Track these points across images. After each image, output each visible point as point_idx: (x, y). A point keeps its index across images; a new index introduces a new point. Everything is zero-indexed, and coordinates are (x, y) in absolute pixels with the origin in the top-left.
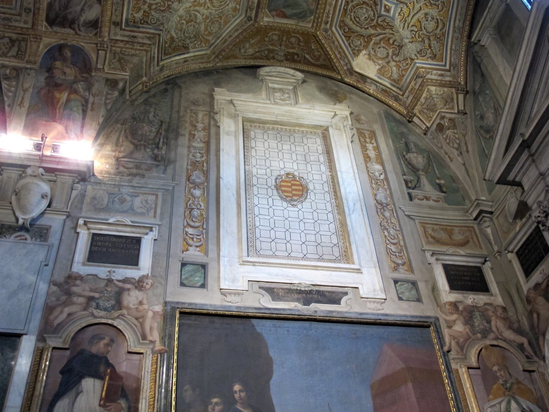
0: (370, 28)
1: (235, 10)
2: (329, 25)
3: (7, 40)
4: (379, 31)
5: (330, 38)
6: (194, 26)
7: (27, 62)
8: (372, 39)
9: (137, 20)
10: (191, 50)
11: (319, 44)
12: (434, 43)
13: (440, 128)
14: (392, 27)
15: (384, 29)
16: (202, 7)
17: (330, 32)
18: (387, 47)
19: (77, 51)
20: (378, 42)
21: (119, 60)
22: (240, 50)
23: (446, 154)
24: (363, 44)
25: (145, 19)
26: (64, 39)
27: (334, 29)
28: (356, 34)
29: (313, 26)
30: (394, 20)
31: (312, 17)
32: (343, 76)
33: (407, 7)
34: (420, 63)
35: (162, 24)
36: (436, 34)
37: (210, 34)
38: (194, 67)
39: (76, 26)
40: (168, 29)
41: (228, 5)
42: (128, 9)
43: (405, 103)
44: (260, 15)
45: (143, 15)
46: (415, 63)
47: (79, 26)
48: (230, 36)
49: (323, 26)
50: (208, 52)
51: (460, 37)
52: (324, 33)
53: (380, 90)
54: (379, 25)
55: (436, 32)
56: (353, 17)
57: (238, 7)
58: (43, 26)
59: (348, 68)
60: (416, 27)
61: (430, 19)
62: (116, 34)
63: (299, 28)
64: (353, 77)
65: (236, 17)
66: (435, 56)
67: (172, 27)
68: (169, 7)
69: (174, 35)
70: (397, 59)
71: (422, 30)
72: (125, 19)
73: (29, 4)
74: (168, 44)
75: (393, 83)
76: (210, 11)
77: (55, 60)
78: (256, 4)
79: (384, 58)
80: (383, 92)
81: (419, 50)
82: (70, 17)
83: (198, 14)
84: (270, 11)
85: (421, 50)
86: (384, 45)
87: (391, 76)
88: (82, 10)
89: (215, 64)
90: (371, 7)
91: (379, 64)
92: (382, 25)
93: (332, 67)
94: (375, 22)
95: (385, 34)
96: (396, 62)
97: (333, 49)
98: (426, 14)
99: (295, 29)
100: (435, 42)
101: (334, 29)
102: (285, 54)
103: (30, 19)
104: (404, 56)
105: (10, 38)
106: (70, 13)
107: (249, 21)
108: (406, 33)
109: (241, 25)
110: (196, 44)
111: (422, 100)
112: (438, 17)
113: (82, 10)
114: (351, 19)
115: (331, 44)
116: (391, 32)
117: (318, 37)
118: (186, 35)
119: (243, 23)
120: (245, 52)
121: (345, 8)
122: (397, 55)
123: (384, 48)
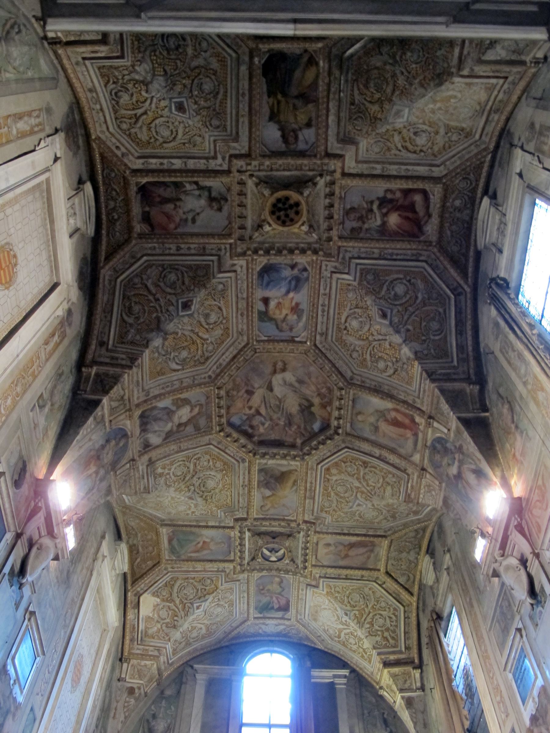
1: (169, 513)
3: (122, 393)
7: (111, 421)
9: (156, 471)
12: (184, 643)
13: (131, 691)
14: (186, 615)
15: (183, 610)
21: (125, 481)
23: (116, 709)
26: (132, 434)
27: (169, 574)
29: (167, 560)
31: (174, 558)
35: (157, 489)
43: (133, 648)
44: (168, 528)
49: (169, 566)
58: (138, 413)
62: (142, 464)
68: (169, 486)
70: (164, 628)
73: (153, 392)
77: (115, 439)
82: (149, 427)
84: (172, 532)
87: (149, 628)
91: (153, 615)
94: (186, 601)
98: (201, 629)
103: (142, 399)
105: (124, 395)
108: (186, 626)
109: (155, 516)
111: (143, 663)
113: (156, 432)
122: (167, 627)
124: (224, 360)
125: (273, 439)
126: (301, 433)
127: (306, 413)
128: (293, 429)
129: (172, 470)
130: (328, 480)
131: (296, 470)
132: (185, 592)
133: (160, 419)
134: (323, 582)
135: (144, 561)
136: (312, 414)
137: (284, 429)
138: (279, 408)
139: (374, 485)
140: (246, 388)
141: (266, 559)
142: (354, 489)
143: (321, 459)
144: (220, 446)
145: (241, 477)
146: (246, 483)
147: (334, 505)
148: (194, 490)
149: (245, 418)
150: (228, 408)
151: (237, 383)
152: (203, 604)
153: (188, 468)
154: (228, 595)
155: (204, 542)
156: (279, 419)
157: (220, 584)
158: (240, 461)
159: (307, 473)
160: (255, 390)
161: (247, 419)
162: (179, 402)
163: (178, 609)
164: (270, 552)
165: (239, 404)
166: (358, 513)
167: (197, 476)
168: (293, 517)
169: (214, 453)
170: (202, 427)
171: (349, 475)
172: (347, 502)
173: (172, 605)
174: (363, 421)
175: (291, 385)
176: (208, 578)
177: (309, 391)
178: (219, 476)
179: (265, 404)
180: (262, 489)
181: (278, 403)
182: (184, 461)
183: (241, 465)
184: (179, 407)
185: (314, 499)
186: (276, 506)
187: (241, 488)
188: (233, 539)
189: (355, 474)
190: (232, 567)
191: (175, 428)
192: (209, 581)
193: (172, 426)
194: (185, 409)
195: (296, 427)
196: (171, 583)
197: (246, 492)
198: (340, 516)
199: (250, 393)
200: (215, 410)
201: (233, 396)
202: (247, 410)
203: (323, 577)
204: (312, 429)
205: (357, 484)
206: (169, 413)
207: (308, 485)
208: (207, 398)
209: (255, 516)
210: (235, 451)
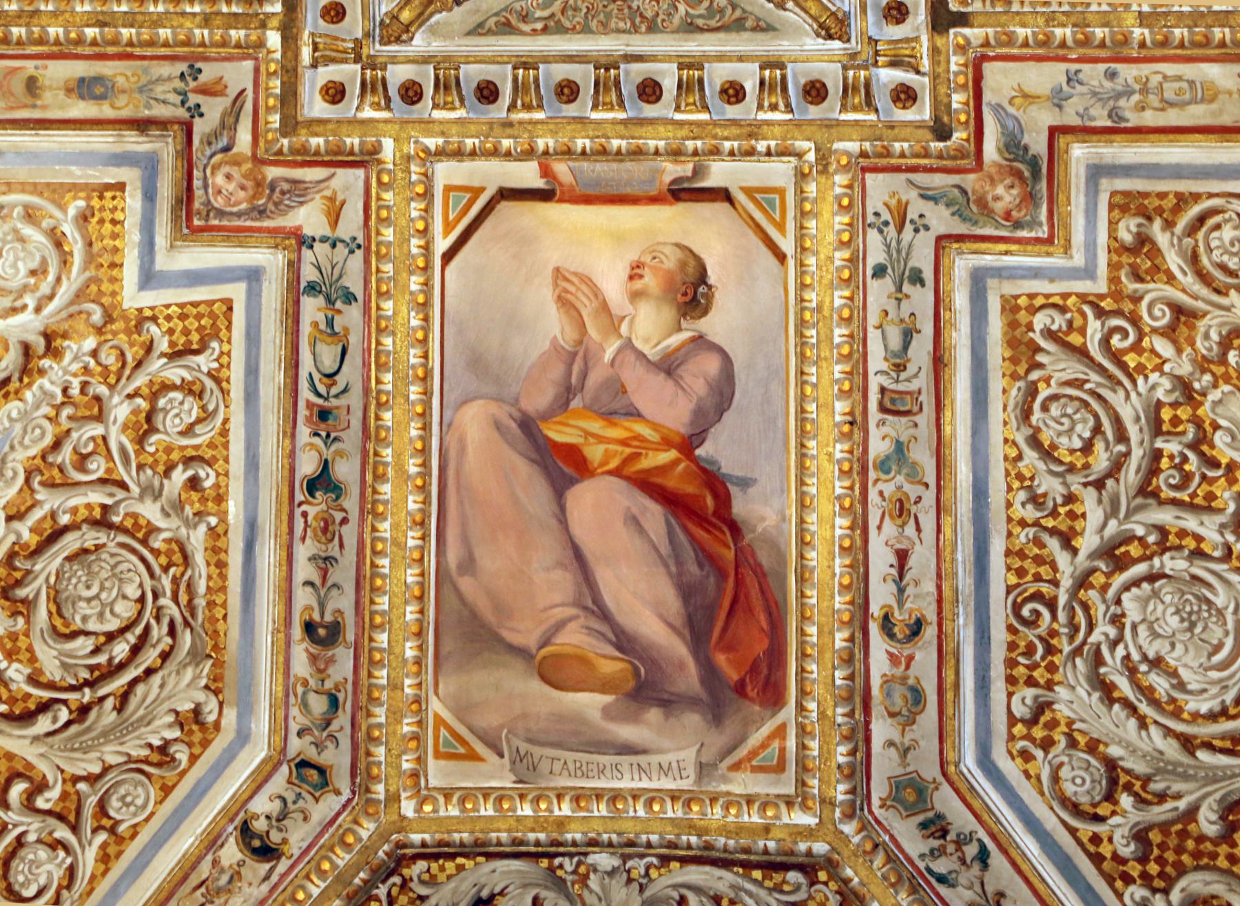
134: (253, 276)
203: (294, 267)
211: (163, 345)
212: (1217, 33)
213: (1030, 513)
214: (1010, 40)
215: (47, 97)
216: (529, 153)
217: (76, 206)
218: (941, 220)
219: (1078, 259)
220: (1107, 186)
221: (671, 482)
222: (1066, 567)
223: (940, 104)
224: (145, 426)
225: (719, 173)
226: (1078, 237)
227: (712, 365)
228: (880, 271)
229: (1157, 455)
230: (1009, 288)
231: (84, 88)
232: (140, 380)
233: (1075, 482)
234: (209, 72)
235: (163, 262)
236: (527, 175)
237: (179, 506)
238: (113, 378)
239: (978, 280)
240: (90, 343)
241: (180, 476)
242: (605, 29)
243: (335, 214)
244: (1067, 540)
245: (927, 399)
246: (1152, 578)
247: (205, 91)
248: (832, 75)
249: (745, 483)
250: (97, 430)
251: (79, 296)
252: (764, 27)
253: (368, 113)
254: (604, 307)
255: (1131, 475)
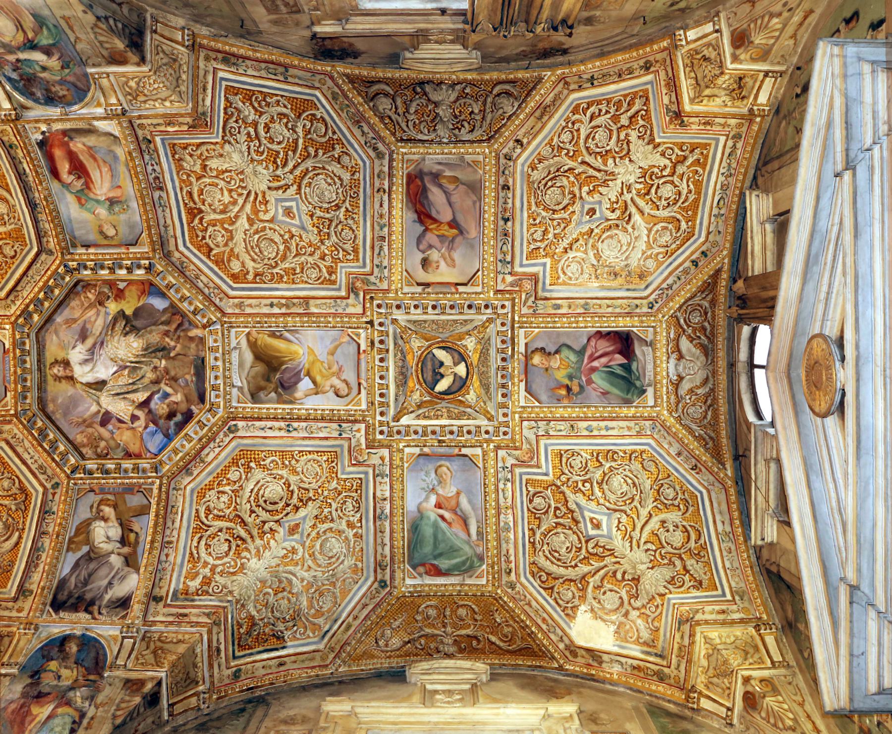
0: (579, 565)
1: (355, 570)
2: (513, 574)
4: (597, 565)
5: (523, 597)
6: (289, 600)
8: (588, 583)
9: (192, 590)
10: (289, 644)
11: (507, 611)
12: (690, 563)
14: (612, 552)
16: (299, 567)
17: (518, 587)
18: (615, 588)
19: (88, 643)
20: (600, 584)
22: (376, 642)
24: (577, 595)
25: (205, 588)
27: (523, 579)
28: (561, 580)
29: (488, 581)
30: (611, 539)
32: (562, 662)
33: (628, 516)
34: (675, 597)
36: (690, 549)
37: (319, 613)
38: (299, 674)
39: (96, 608)
40: (240, 600)
41: (343, 561)
42: (179, 576)
44: (399, 575)
45: (202, 582)
46: (669, 599)
47: (100, 608)
48: (355, 618)
49: (505, 578)
50: (321, 646)
51: (733, 548)
52: (509, 590)
53: (629, 670)
54: (591, 554)
55: (689, 546)
56: (547, 553)
57: (360, 565)
59: (566, 646)
60: (652, 543)
61: (671, 528)
63: (466, 588)
64: (579, 659)
65: (360, 583)
66: (701, 583)
67: (249, 597)
69: (254, 613)
70: (638, 604)
71: (664, 547)
72: (174, 592)
74: (245, 627)
75: (645, 649)
76: (313, 573)
78: (388, 558)
79: (618, 609)
80: (636, 672)
81: (668, 578)
83: (294, 579)
84: (414, 567)
85: (673, 578)
86: (610, 586)
87: (639, 637)
88: (110, 584)
89: (337, 670)
90: (570, 528)
91: (613, 623)
92: (596, 554)
93: (540, 650)
94: (584, 551)
95: (606, 566)
96: (638, 609)
97: (532, 615)
98: (663, 522)
99: (460, 591)
100: (693, 562)
101: (523, 579)
102: (455, 640)
104: (647, 593)
106: (91, 590)
107: (383, 587)
110: (296, 632)
112: (685, 523)
113: (110, 584)
114: (547, 558)
115: (526, 607)
116: (614, 560)
117: (500, 598)
118: (277, 614)
119: (374, 592)
120: (387, 645)
121: (532, 540)
123: (611, 591)
124: (36, 461)
125: (194, 379)
126: (176, 329)
127: (138, 323)
128: (172, 344)
129: (210, 560)
130: (256, 275)
131: (248, 334)
132: (563, 551)
133: (90, 575)
135: (495, 628)
136: (137, 312)
137: (173, 358)
138: (135, 368)
139: (226, 193)
140: (96, 426)
141: (461, 384)
142: (255, 227)
143: (216, 291)
144: (195, 473)
145: (270, 433)
146: (282, 424)
147: (310, 259)
148: (276, 522)
149: (152, 427)
150: (128, 455)
151: (85, 440)
152: (587, 514)
153: (220, 530)
154: (577, 462)
155: (439, 506)
156: (155, 368)
157: (545, 478)
158: (232, 436)
159: (250, 314)
160: (103, 411)
161: (155, 423)
162: (75, 540)
163: (602, 568)
164: (442, 376)
165: (125, 437)
166: (319, 213)
167: (246, 518)
168: (358, 335)
169: (207, 482)
170: (145, 502)
171: (231, 238)
172: (292, 237)
173: (593, 581)
174: (115, 227)
175: (91, 351)
176: (531, 501)
177: (98, 322)
178: (258, 474)
179: (128, 393)
180: (298, 394)
181: (126, 372)
182: (201, 538)
183: (239, 434)
184: (88, 541)
185: (307, 299)
186: (335, 368)
187: (294, 434)
188: (426, 450)
189: (226, 230)
190: (501, 453)
191: (126, 550)
192: (537, 500)
193: (119, 554)
194: (96, 529)
195: (167, 339)
196: (544, 578)
197: (304, 424)
198: (335, 246)
199: (106, 419)
200: (114, 478)
201: (108, 447)
202: (136, 424)
204: (165, 310)
205: (242, 223)
206: (93, 557)
207: (276, 310)
208: (92, 490)
209: (364, 406)
210: (212, 445)
211: (541, 250)
212: (314, 319)
213: (354, 216)
214: (357, 318)
215: (567, 304)
216: (460, 293)
217: (560, 281)
218: (372, 279)
219: (344, 270)
220: (337, 286)
221: (430, 221)
222: (347, 204)
223: (372, 304)
224: (545, 232)
225: (419, 289)
226: (343, 275)
227: (421, 247)
228: (385, 267)
229: (328, 229)
230: (358, 264)
231: (558, 307)
232: (546, 242)
233: (345, 223)
234: (531, 311)
235: (541, 268)
236: (461, 289)
237: (538, 215)
238: (552, 243)
239: (364, 266)
240: (557, 251)
241: (537, 221)
242: (444, 321)
243: (503, 280)
244: (347, 210)
245: (376, 240)
246: (330, 202)
247: (532, 307)
248: (395, 311)
249: (414, 221)
250: (556, 232)
251: (560, 261)
252: (409, 321)
253: (496, 302)
254: (445, 259)
255: (334, 224)
